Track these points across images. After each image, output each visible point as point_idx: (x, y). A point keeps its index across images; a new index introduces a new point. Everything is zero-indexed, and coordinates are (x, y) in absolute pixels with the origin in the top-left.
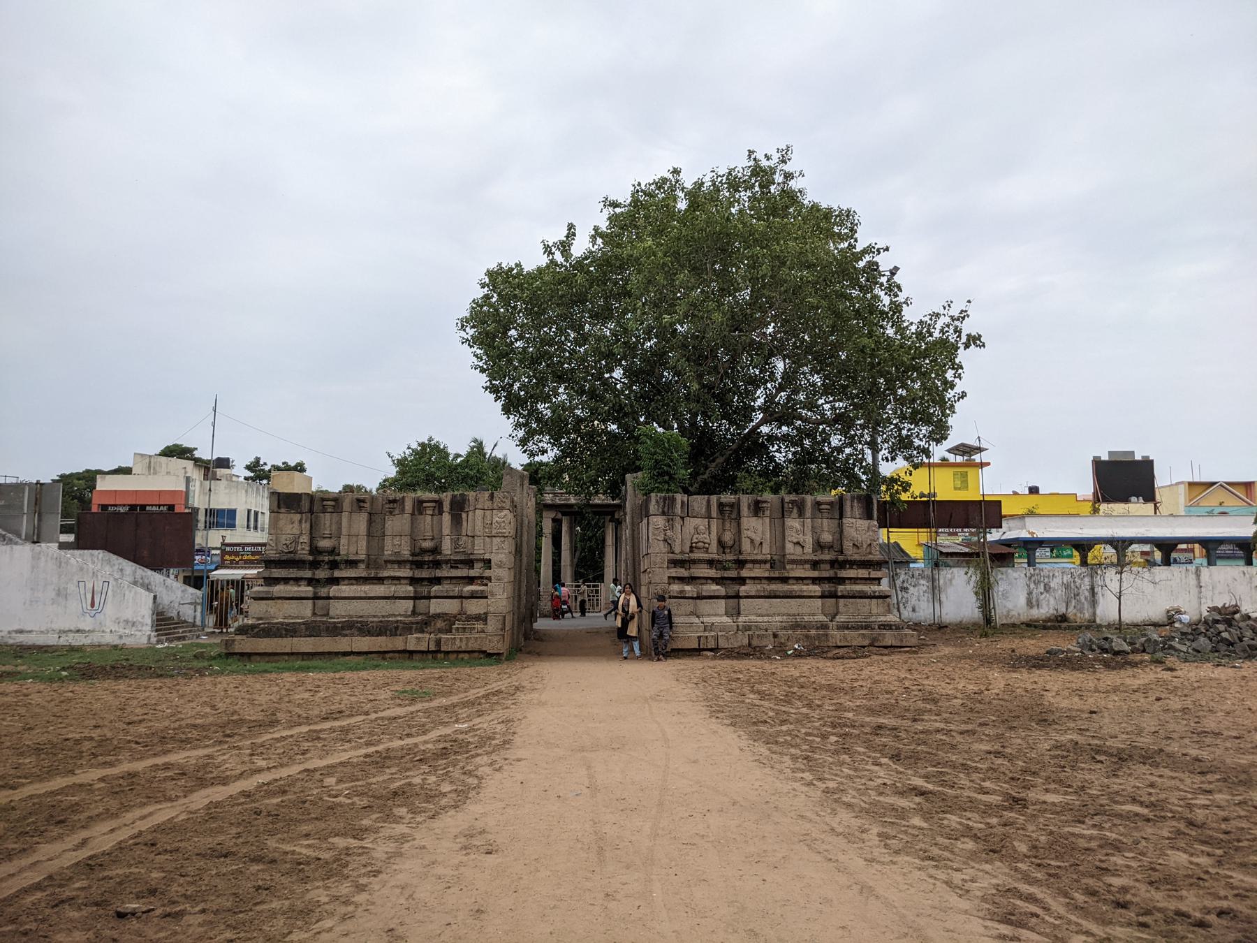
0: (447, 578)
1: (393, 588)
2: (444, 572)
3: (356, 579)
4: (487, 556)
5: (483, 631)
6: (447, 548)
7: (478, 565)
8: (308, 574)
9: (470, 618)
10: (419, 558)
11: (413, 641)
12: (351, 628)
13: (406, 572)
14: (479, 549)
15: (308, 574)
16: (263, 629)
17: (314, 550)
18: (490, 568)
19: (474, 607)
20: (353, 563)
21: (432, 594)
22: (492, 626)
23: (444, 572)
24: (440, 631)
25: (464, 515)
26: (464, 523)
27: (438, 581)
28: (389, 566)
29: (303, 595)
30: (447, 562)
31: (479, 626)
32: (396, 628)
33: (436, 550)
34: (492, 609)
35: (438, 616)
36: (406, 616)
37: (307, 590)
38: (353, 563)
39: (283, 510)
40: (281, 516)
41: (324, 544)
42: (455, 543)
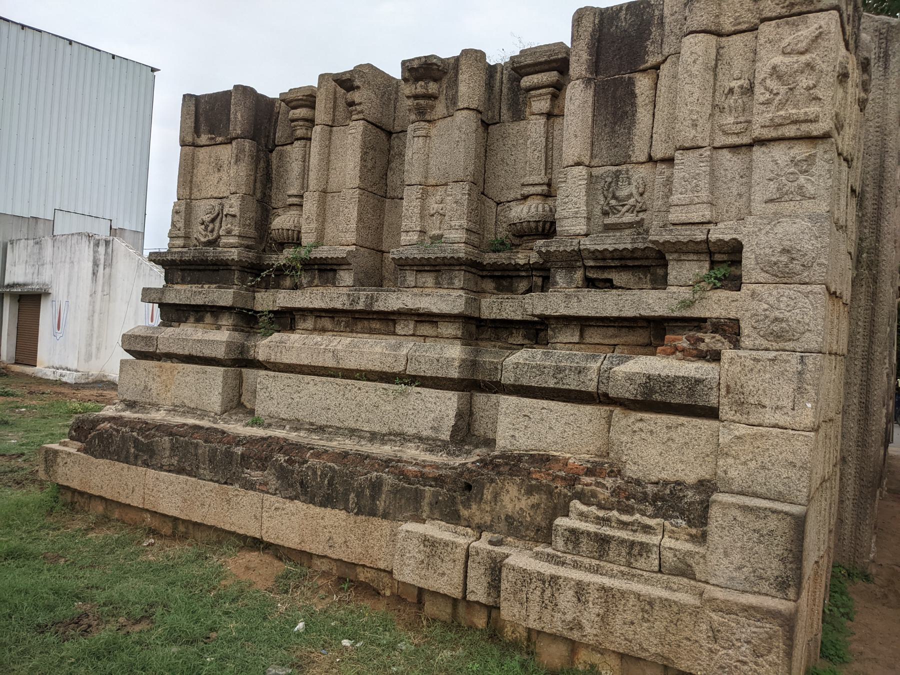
0: (567, 321)
1: (408, 347)
2: (562, 299)
3: (332, 313)
4: (721, 233)
5: (685, 571)
6: (574, 213)
7: (685, 272)
8: (225, 296)
9: (634, 495)
10: (502, 258)
11: (415, 551)
12: (263, 463)
13: (448, 299)
14: (686, 202)
15: (225, 296)
16: (100, 435)
17: (262, 236)
18: (734, 282)
19: (659, 450)
20: (325, 270)
21: (508, 378)
22: (733, 558)
23: (562, 299)
24: (514, 527)
25: (642, 83)
26: (643, 115)
27: (537, 330)
28: (410, 278)
29: (208, 352)
30: (573, 260)
31: (672, 540)
32: (376, 486)
33: (547, 228)
34: (736, 473)
35: (513, 465)
36: (432, 444)
37: (218, 337)
38: (325, 270)
39: (204, 139)
40: (202, 153)
41: (282, 222)
42: (605, 191)
